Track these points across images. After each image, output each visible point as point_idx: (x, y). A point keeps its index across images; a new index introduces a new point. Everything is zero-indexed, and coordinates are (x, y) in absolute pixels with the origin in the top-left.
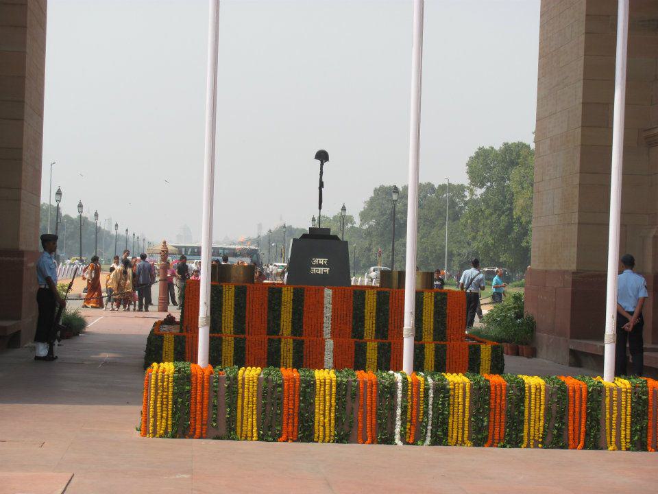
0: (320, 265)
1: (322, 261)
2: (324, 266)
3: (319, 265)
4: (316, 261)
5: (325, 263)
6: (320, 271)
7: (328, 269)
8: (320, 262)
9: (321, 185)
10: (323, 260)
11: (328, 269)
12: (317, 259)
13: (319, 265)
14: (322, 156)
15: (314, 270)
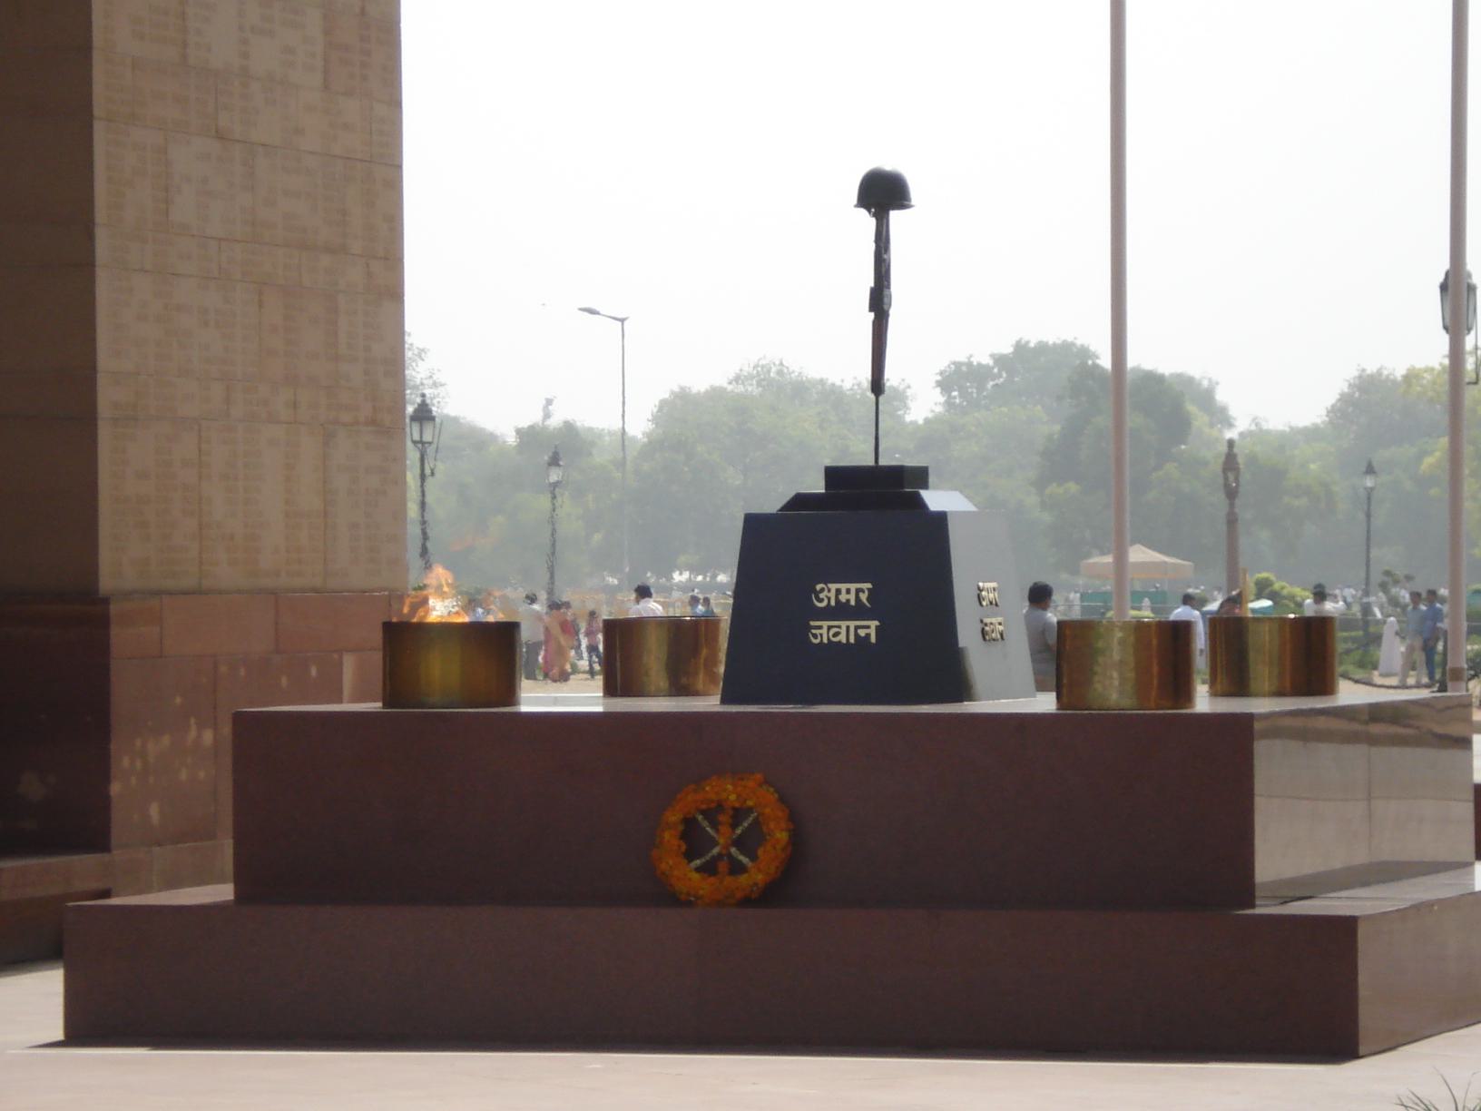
0: (842, 614)
1: (850, 591)
2: (856, 612)
3: (840, 611)
4: (829, 593)
5: (864, 597)
6: (844, 631)
7: (874, 624)
8: (843, 598)
9: (879, 301)
10: (853, 587)
11: (874, 624)
12: (833, 587)
13: (840, 611)
14: (883, 193)
15: (824, 632)
